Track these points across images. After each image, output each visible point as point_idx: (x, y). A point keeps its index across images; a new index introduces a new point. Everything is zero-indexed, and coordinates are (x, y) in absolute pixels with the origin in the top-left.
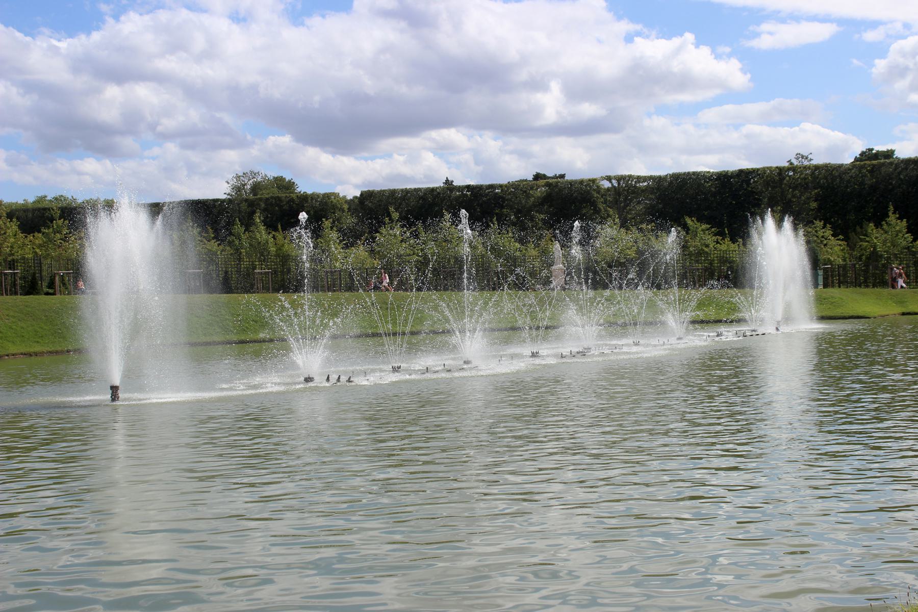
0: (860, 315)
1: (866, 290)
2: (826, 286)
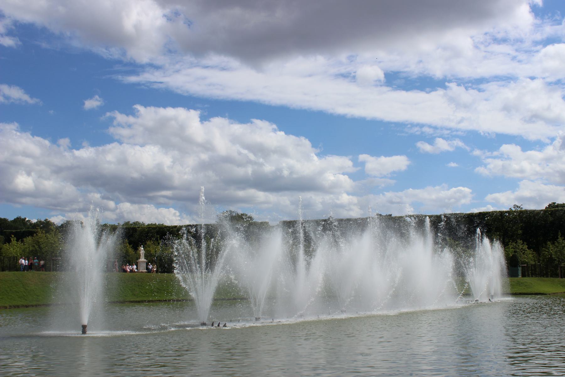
0: (542, 292)
1: (545, 279)
2: (524, 275)
